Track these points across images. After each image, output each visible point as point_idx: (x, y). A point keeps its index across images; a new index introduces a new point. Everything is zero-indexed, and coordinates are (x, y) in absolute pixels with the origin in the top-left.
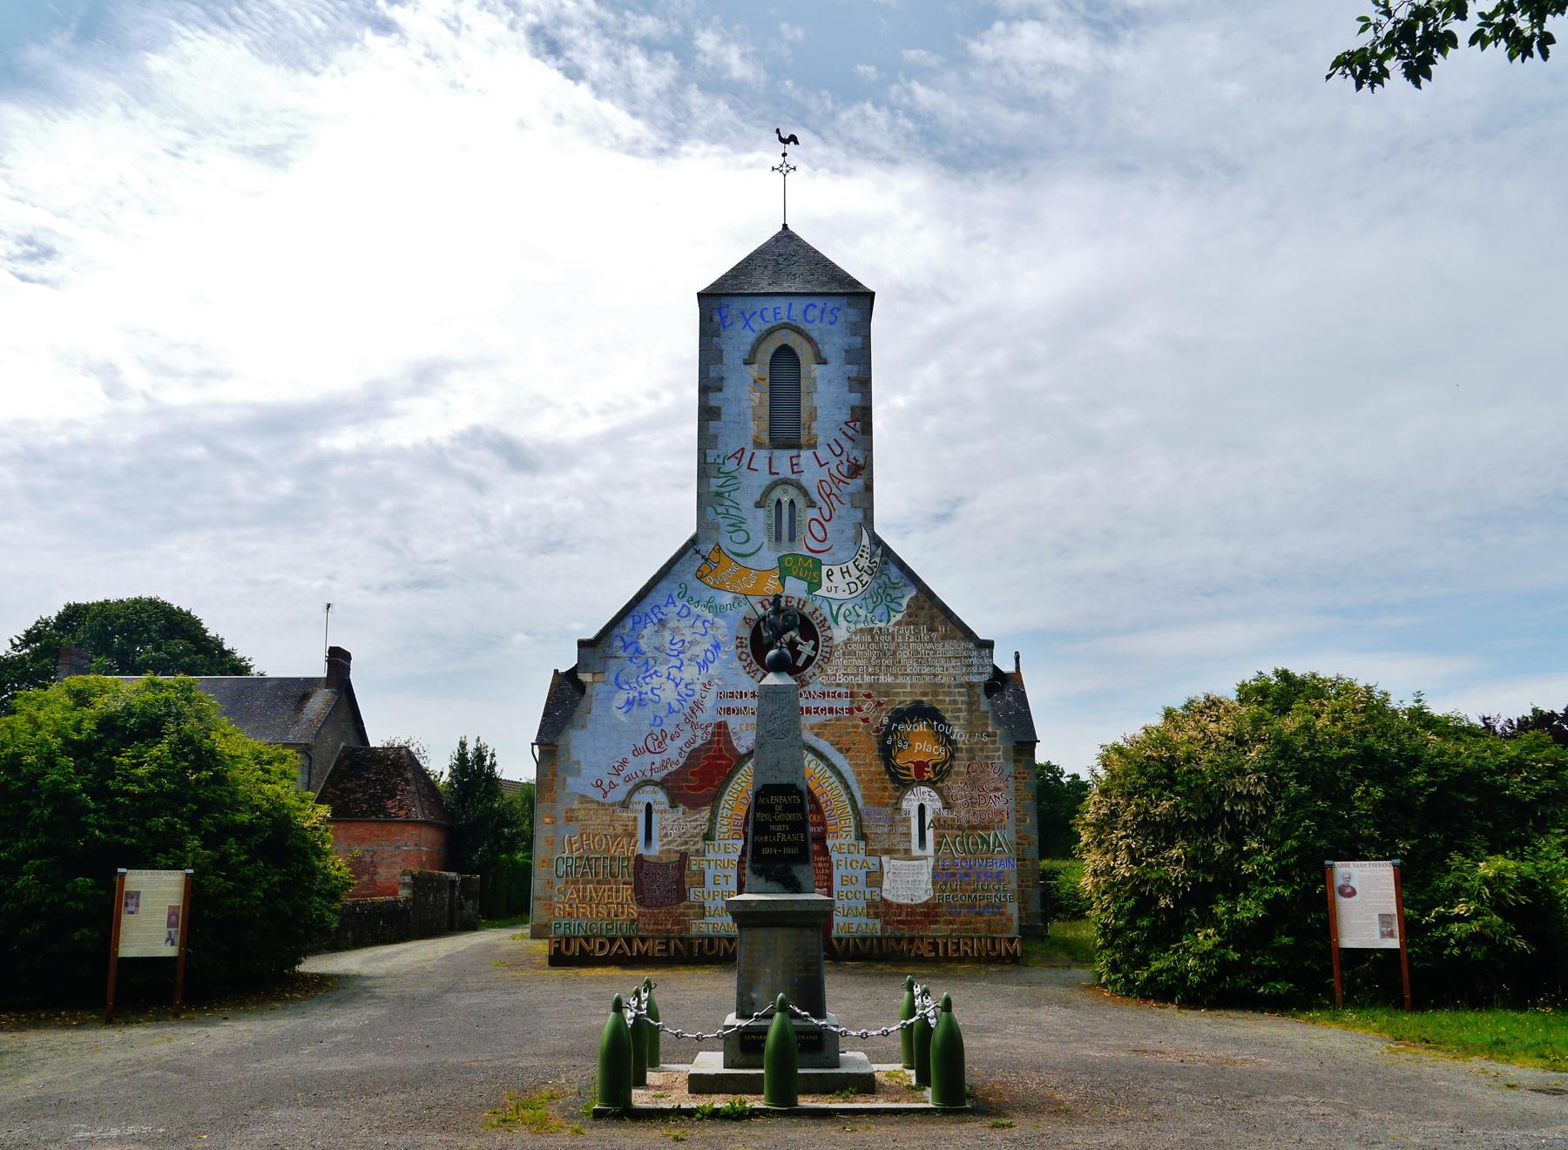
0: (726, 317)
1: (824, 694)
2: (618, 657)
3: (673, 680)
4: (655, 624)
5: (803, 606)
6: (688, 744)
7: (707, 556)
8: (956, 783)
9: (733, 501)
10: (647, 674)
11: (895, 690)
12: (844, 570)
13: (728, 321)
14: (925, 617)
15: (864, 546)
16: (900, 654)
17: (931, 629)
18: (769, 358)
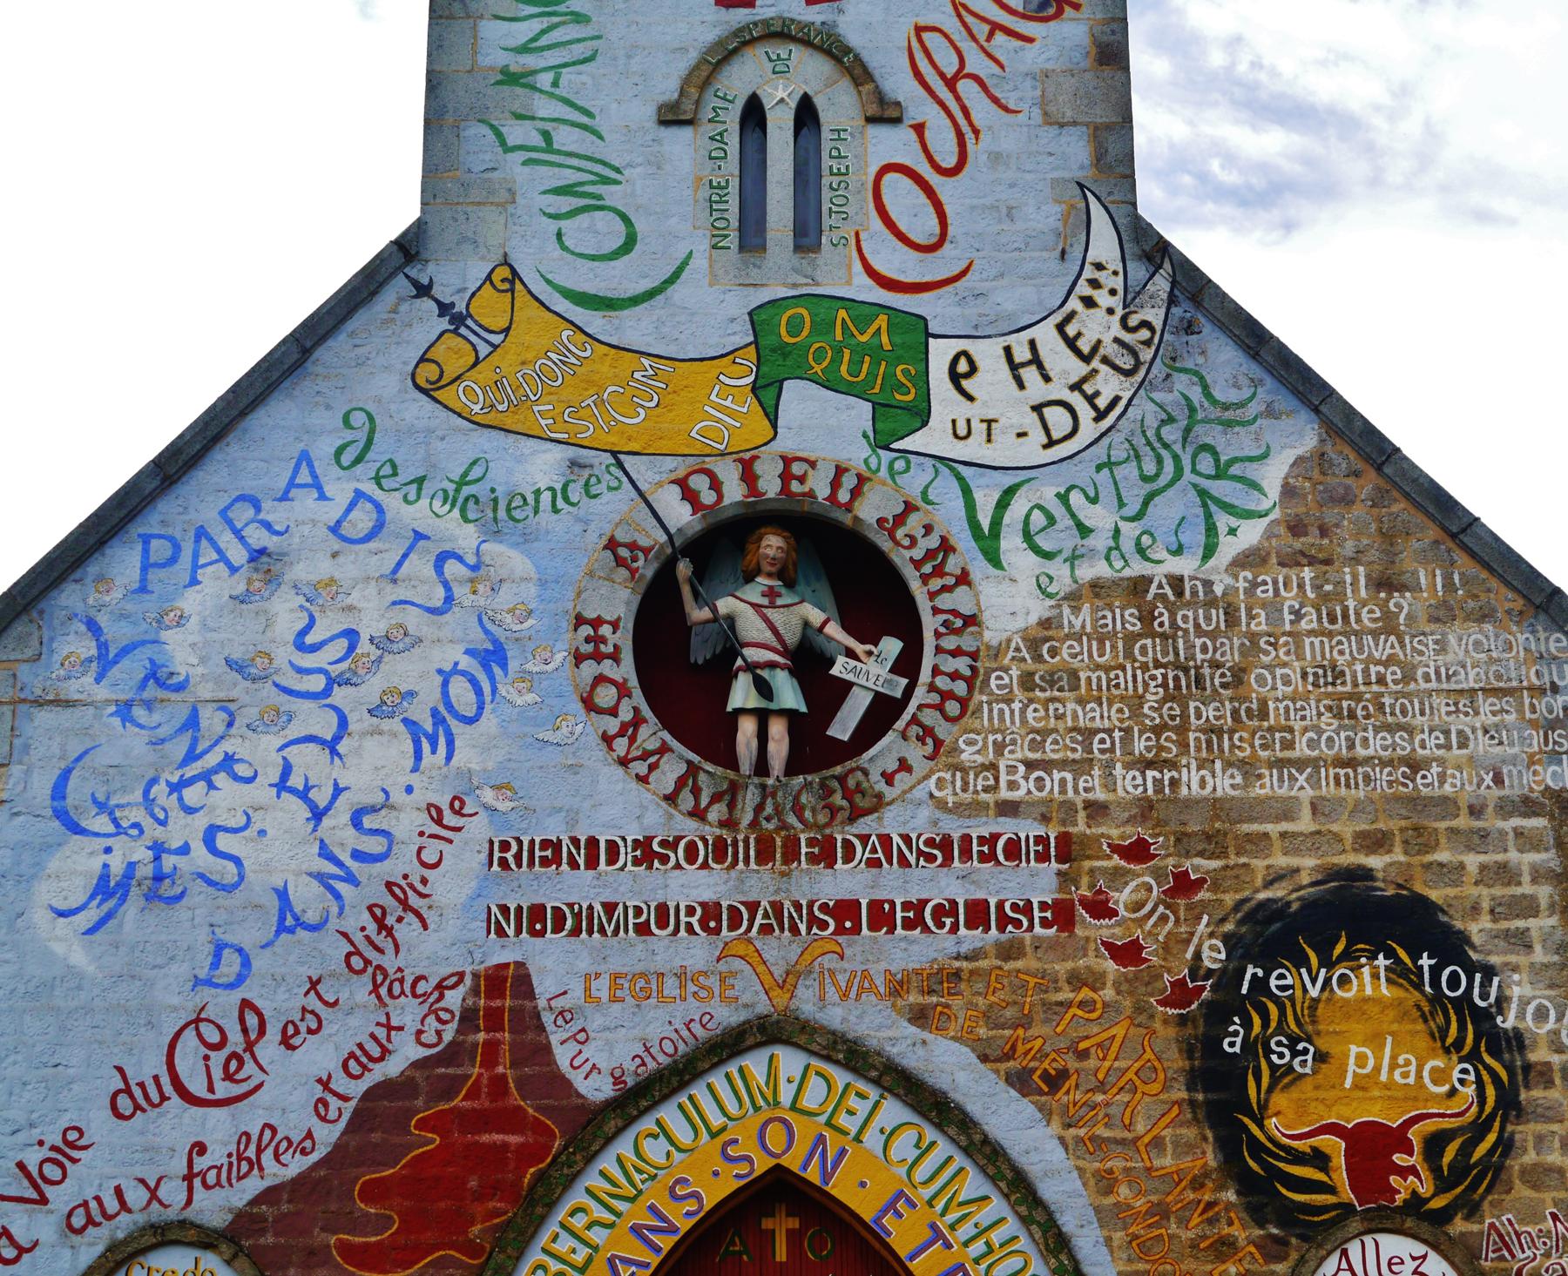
1: (945, 844)
2: (68, 704)
3: (303, 795)
4: (234, 570)
5: (856, 492)
6: (357, 1062)
7: (460, 307)
8: (1537, 1218)
9: (567, 102)
10: (190, 772)
11: (1246, 828)
12: (1022, 354)
14: (1357, 535)
15: (1099, 267)
16: (1261, 680)
17: (1386, 583)
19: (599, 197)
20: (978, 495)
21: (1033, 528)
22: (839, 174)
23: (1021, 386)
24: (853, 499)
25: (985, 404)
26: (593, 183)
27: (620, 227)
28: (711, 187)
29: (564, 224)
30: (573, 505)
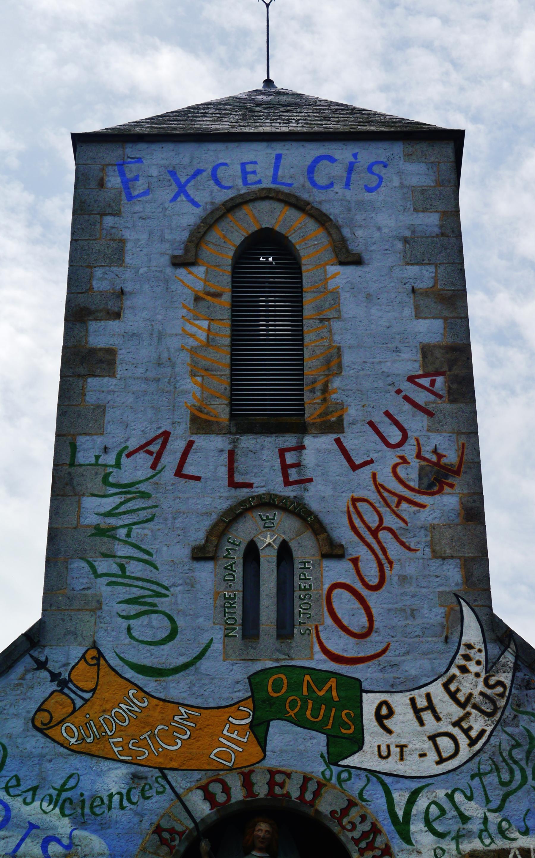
0: (136, 178)
12: (422, 703)
13: (140, 187)
15: (469, 647)
18: (231, 254)
19: (154, 605)
20: (396, 795)
21: (431, 817)
22: (305, 589)
23: (421, 723)
24: (315, 798)
25: (399, 735)
26: (150, 596)
27: (167, 623)
28: (225, 598)
29: (131, 622)
30: (133, 804)
